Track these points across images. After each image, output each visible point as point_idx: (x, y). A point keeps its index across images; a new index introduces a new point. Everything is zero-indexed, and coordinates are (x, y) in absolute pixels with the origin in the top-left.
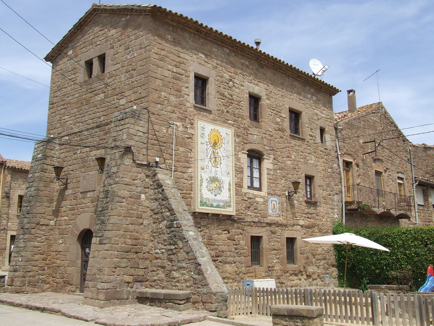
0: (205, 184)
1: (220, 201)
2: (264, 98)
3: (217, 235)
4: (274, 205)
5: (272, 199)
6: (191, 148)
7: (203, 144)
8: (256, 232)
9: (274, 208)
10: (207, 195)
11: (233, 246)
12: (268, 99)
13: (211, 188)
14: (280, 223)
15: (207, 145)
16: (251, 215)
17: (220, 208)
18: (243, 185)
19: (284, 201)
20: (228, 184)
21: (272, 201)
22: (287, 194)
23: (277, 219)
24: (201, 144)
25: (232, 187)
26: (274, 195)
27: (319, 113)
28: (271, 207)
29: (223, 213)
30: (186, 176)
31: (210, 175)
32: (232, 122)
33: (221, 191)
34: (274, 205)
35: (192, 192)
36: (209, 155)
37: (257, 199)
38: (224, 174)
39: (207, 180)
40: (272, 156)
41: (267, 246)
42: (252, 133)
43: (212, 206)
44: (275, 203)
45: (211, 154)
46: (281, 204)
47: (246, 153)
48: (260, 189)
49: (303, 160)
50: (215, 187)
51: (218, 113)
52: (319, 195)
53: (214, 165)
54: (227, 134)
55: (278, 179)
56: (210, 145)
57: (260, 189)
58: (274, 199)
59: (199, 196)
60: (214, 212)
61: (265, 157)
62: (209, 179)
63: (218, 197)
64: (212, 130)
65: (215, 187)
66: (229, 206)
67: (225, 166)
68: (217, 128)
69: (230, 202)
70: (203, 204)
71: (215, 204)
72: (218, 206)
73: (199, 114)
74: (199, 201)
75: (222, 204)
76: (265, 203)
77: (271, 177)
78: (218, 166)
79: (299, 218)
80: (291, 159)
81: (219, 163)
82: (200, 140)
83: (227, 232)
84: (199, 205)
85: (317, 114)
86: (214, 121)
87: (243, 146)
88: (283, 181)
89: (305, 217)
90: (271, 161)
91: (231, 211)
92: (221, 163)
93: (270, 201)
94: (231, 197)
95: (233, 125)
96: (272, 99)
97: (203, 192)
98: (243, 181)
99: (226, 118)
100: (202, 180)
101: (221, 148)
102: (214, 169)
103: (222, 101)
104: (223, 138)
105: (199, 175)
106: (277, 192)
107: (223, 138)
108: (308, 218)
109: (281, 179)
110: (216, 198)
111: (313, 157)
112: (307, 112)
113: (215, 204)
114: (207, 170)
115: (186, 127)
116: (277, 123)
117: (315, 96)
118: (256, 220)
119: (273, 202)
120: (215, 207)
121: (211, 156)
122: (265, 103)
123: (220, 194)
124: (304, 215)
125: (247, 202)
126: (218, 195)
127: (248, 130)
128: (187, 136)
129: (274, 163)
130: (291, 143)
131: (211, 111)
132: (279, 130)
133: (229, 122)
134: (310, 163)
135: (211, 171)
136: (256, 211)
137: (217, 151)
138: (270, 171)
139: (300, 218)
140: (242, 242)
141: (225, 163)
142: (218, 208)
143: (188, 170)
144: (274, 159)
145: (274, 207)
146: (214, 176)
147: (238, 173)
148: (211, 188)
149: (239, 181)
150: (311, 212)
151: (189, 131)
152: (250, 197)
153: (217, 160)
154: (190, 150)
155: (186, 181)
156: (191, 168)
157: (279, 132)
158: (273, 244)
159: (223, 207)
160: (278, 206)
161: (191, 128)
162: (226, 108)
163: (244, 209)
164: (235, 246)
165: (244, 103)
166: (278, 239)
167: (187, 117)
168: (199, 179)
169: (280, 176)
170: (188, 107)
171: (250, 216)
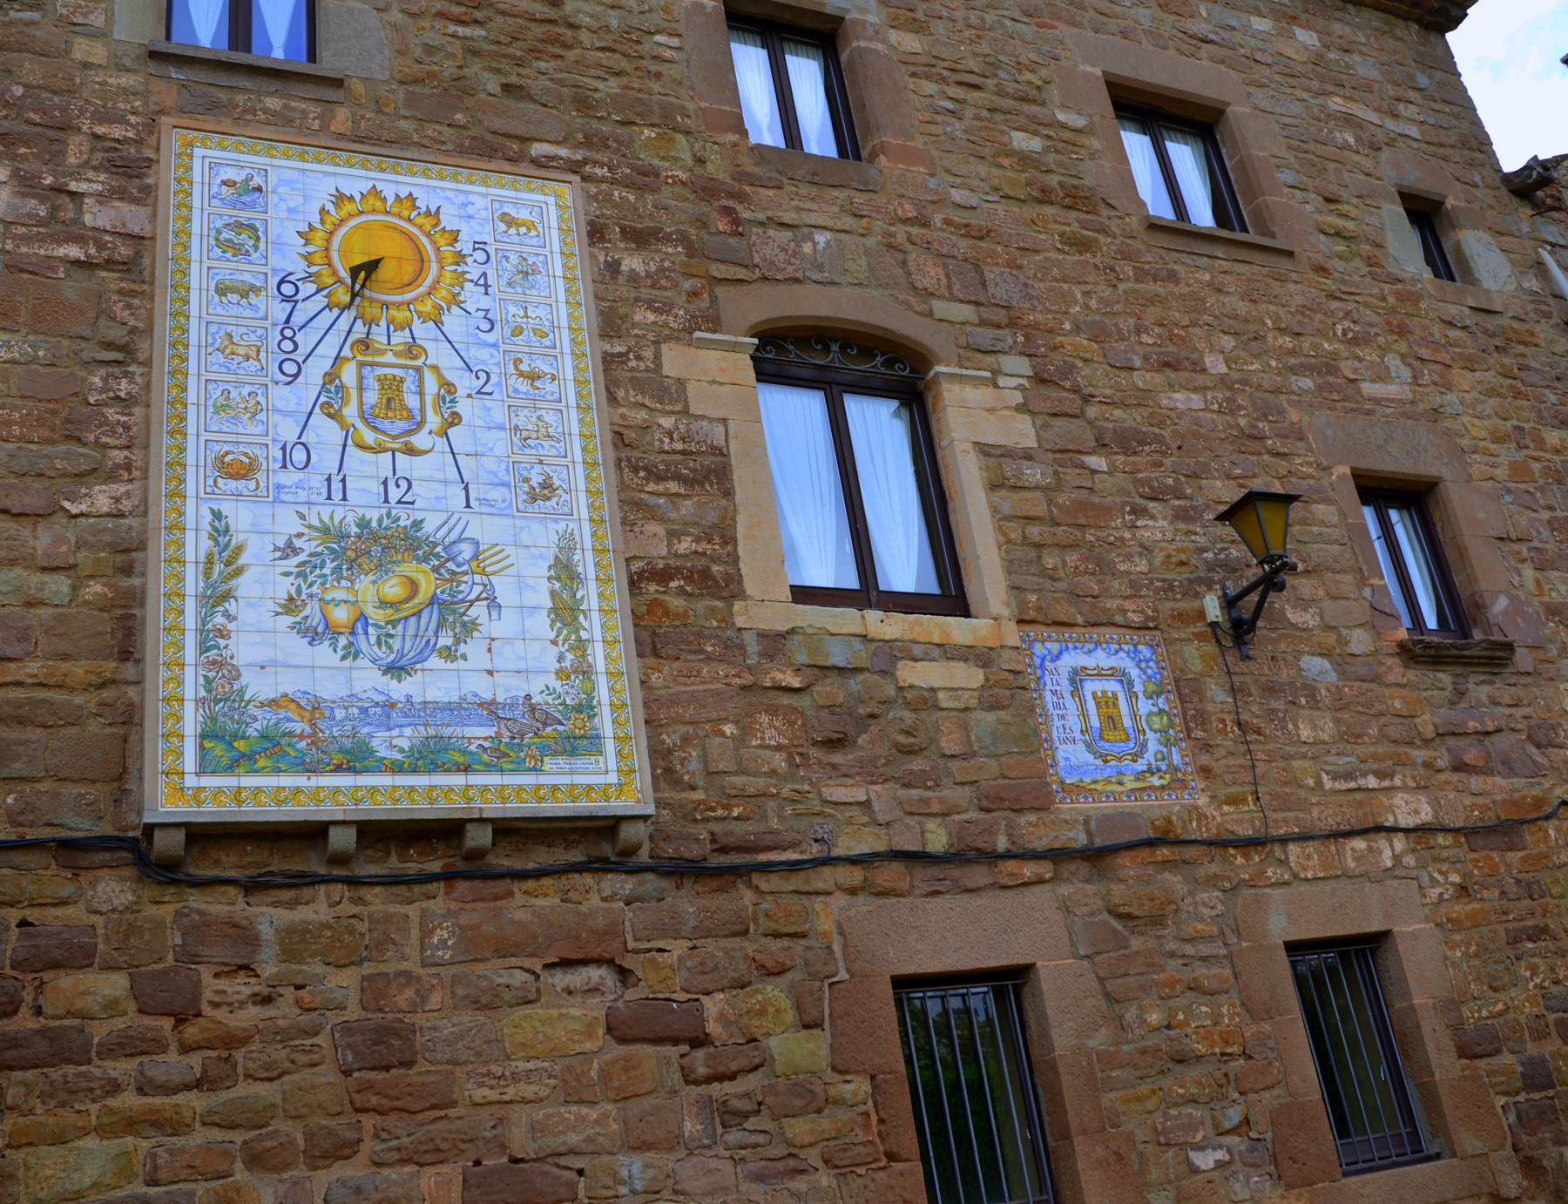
0: (261, 586)
1: (449, 707)
2: (872, 18)
3: (467, 1018)
4: (1106, 703)
5: (1072, 660)
6: (116, 334)
7: (246, 291)
8: (952, 932)
9: (1103, 719)
10: (272, 657)
11: (695, 1091)
12: (917, 27)
13: (341, 615)
14: (1194, 830)
15: (286, 299)
16: (866, 805)
17: (466, 769)
18: (739, 579)
19: (1197, 666)
20: (538, 571)
21: (1077, 677)
22: (1213, 608)
23: (1171, 805)
24: (222, 291)
25: (590, 595)
26: (1096, 633)
27: (1374, 117)
28: (1074, 722)
29: (493, 808)
30: (58, 540)
31: (322, 513)
32: (563, 152)
33: (470, 628)
34: (1106, 703)
35: (129, 670)
36: (317, 369)
37: (915, 674)
38: (496, 494)
39: (289, 550)
40: (1023, 366)
41: (1099, 1040)
42: (788, 217)
43: (355, 759)
44: (1112, 686)
45: (338, 360)
46: (1185, 689)
47: (734, 347)
48: (952, 597)
49: (1307, 383)
50: (383, 604)
51: (411, 100)
52: (1512, 598)
53: (369, 437)
54: (509, 221)
55: (1106, 511)
56: (320, 300)
57: (952, 597)
58: (1101, 659)
59: (192, 686)
60: (381, 808)
61: (940, 368)
62: (308, 546)
63: (435, 683)
64: (340, 198)
65: (383, 604)
66: (579, 744)
67: (500, 443)
68: (394, 183)
69: (586, 708)
70: (227, 744)
71: (391, 742)
72: (428, 757)
73: (213, 107)
74: (191, 722)
75: (480, 732)
76: (1011, 690)
77: (1036, 504)
78: (420, 440)
79: (1372, 782)
80: (1200, 380)
81: (433, 421)
82: (202, 268)
83: (595, 974)
84: (190, 762)
85: (1349, 121)
86: (373, 140)
87: (704, 302)
88: (1157, 527)
89: (1427, 765)
90: (1018, 398)
91: (605, 777)
92: (455, 420)
93: (1057, 680)
94: (585, 671)
95: (574, 167)
96: (940, 28)
97: (243, 649)
98: (730, 540)
99: (497, 124)
100: (226, 559)
101: (454, 322)
102: (366, 471)
103: (461, 30)
104: (465, 246)
105: (196, 513)
106: (1112, 604)
107: (465, 246)
108: (1460, 767)
109: (1138, 512)
110: (399, 689)
111: (1393, 361)
112: (1263, 104)
113: (391, 742)
114: (290, 478)
115: (60, 190)
116: (1025, 160)
117: (1308, 27)
118: (937, 839)
119: (1090, 687)
120: (397, 768)
121: (331, 377)
122: (880, 47)
123: (449, 654)
124: (1419, 755)
125: (802, 702)
126: (434, 662)
127: (741, 197)
128: (74, 252)
129: (1046, 406)
130: (1172, 277)
131: (338, 83)
132: (1045, 197)
133: (538, 149)
134: (1377, 401)
135: (337, 486)
136: (917, 764)
137: (400, 338)
138: (1009, 468)
139: (1381, 775)
140: (793, 1049)
141: (499, 415)
142: (435, 768)
143: (73, 498)
144: (1040, 380)
145: (1112, 721)
146: (373, 515)
147: (673, 487)
148: (341, 615)
149: (685, 545)
150: (1472, 725)
151: (95, 216)
152: (838, 660)
153: (412, 401)
154: (109, 346)
155: (59, 585)
156: (112, 477)
157: (1049, 210)
158: (1154, 1018)
159: (498, 757)
160: (1144, 706)
161: (122, 194)
162: (498, 71)
163: (779, 761)
164: (716, 1089)
165: (675, 42)
166: (1201, 971)
167: (66, 127)
168: (196, 545)
169: (1122, 491)
170: (86, 65)
171: (859, 808)
